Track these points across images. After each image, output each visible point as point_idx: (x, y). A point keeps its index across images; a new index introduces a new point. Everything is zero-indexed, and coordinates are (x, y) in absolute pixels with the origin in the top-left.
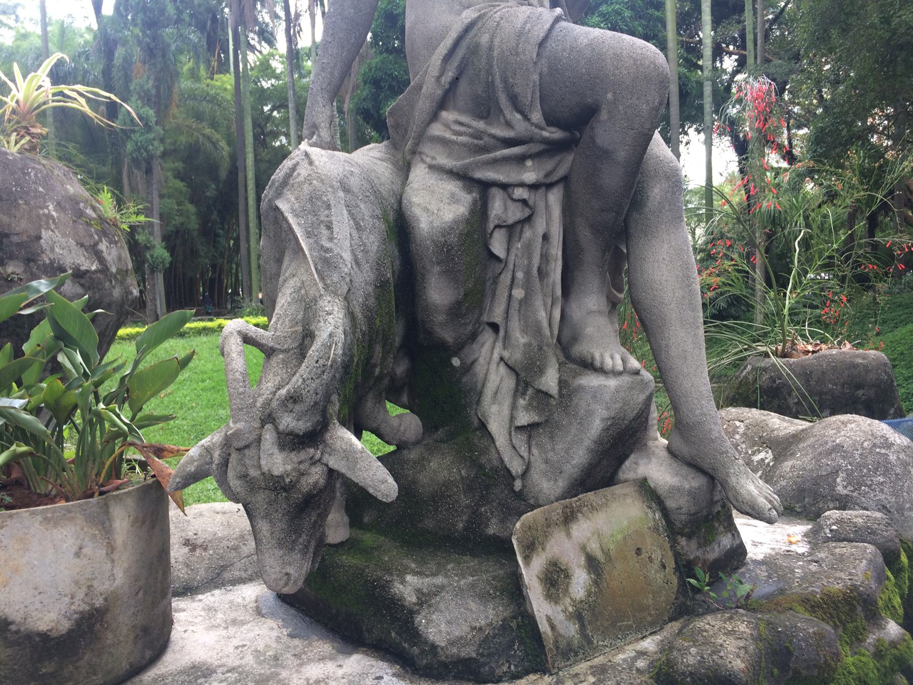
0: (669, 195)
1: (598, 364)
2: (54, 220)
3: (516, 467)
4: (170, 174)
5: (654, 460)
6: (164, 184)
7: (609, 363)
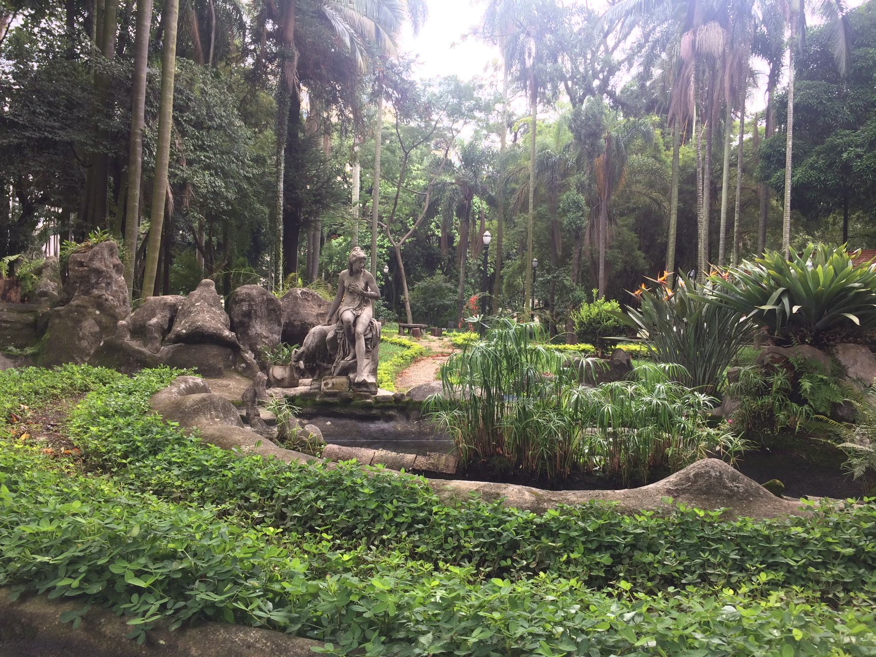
6: (615, 237)
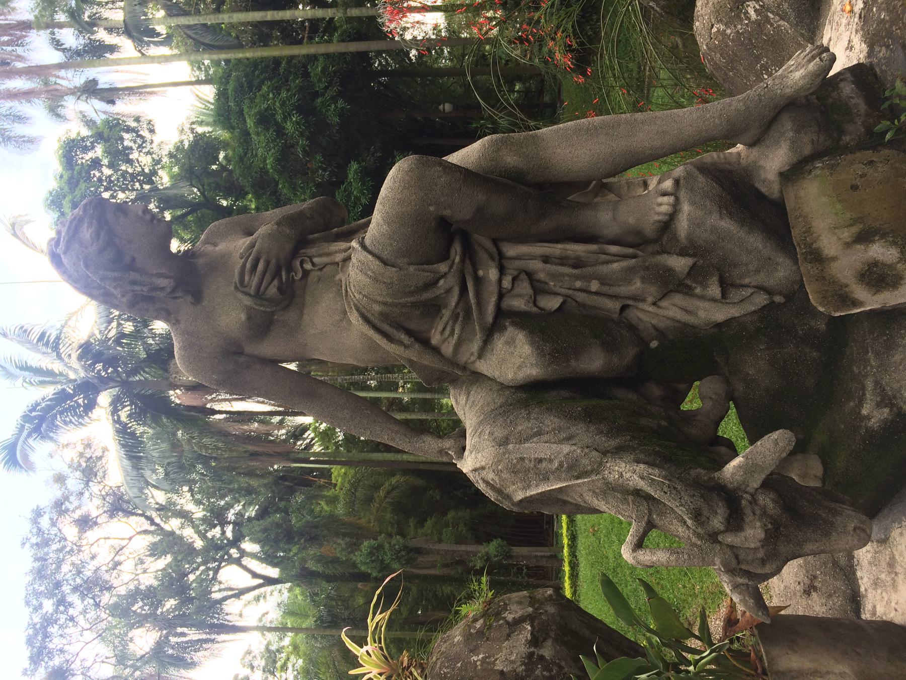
0: (513, 149)
1: (666, 218)
2: (487, 657)
3: (761, 300)
4: (420, 531)
5: (761, 163)
7: (665, 209)
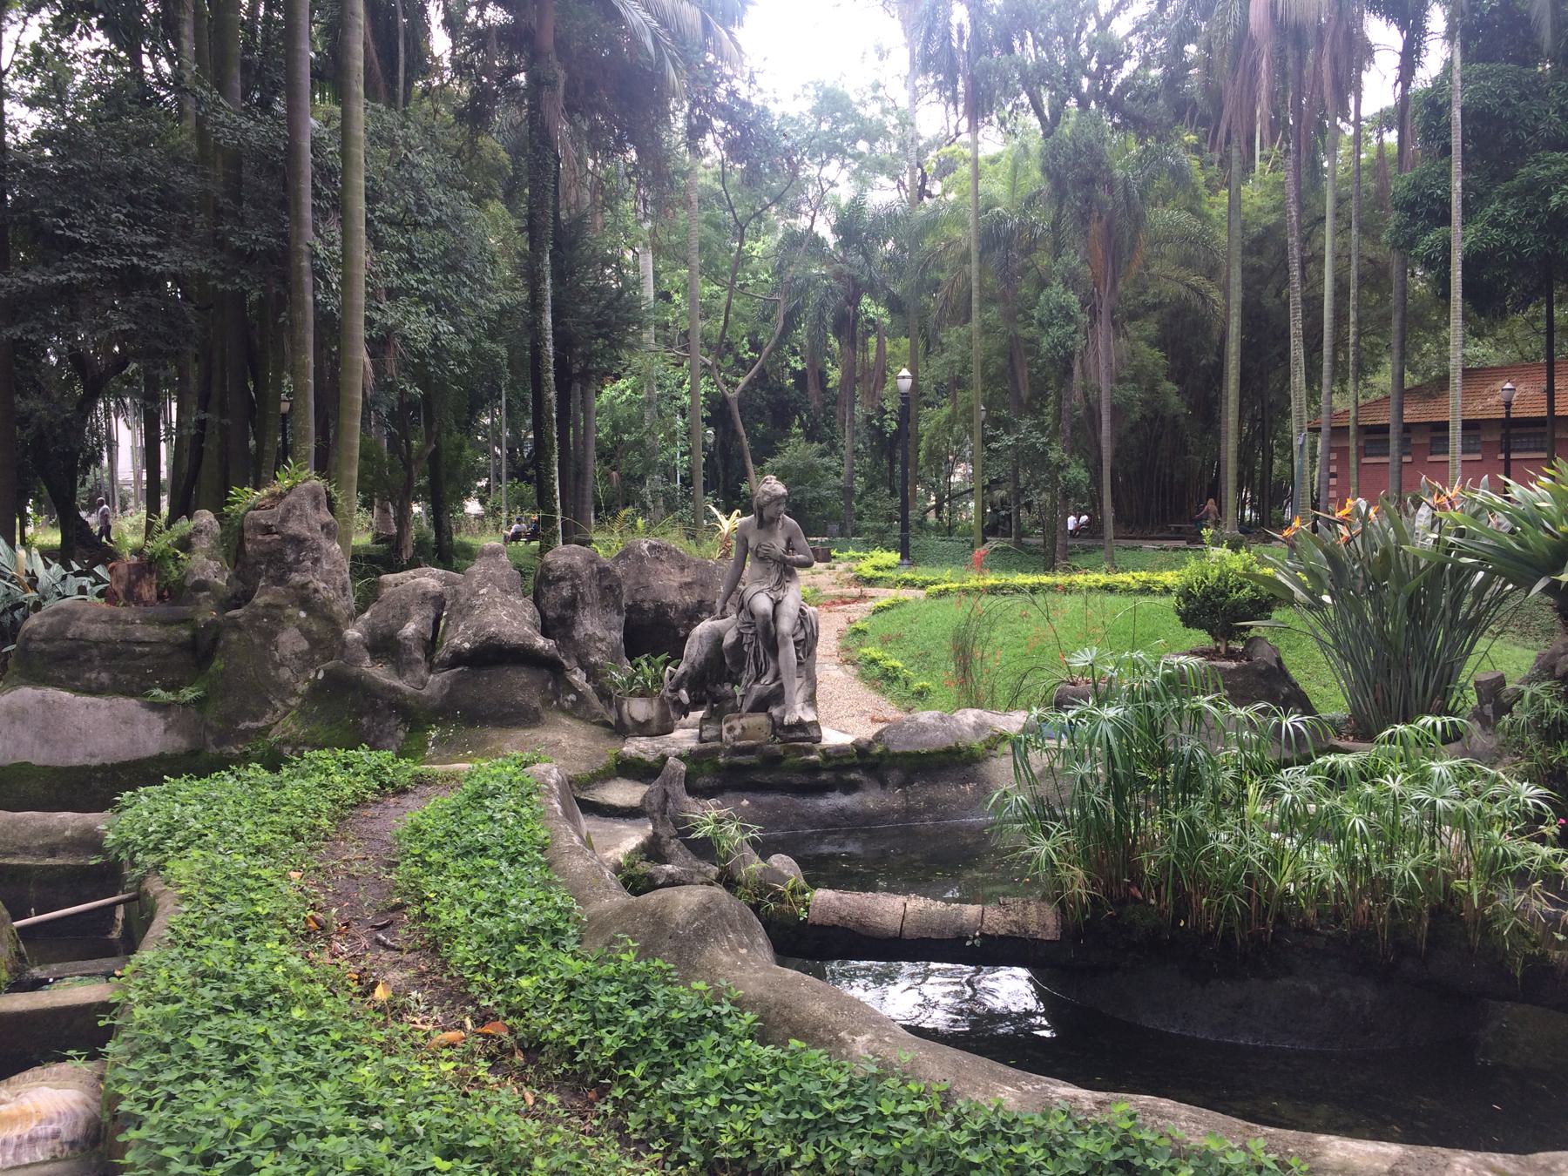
4: (1142, 345)
6: (1125, 361)
